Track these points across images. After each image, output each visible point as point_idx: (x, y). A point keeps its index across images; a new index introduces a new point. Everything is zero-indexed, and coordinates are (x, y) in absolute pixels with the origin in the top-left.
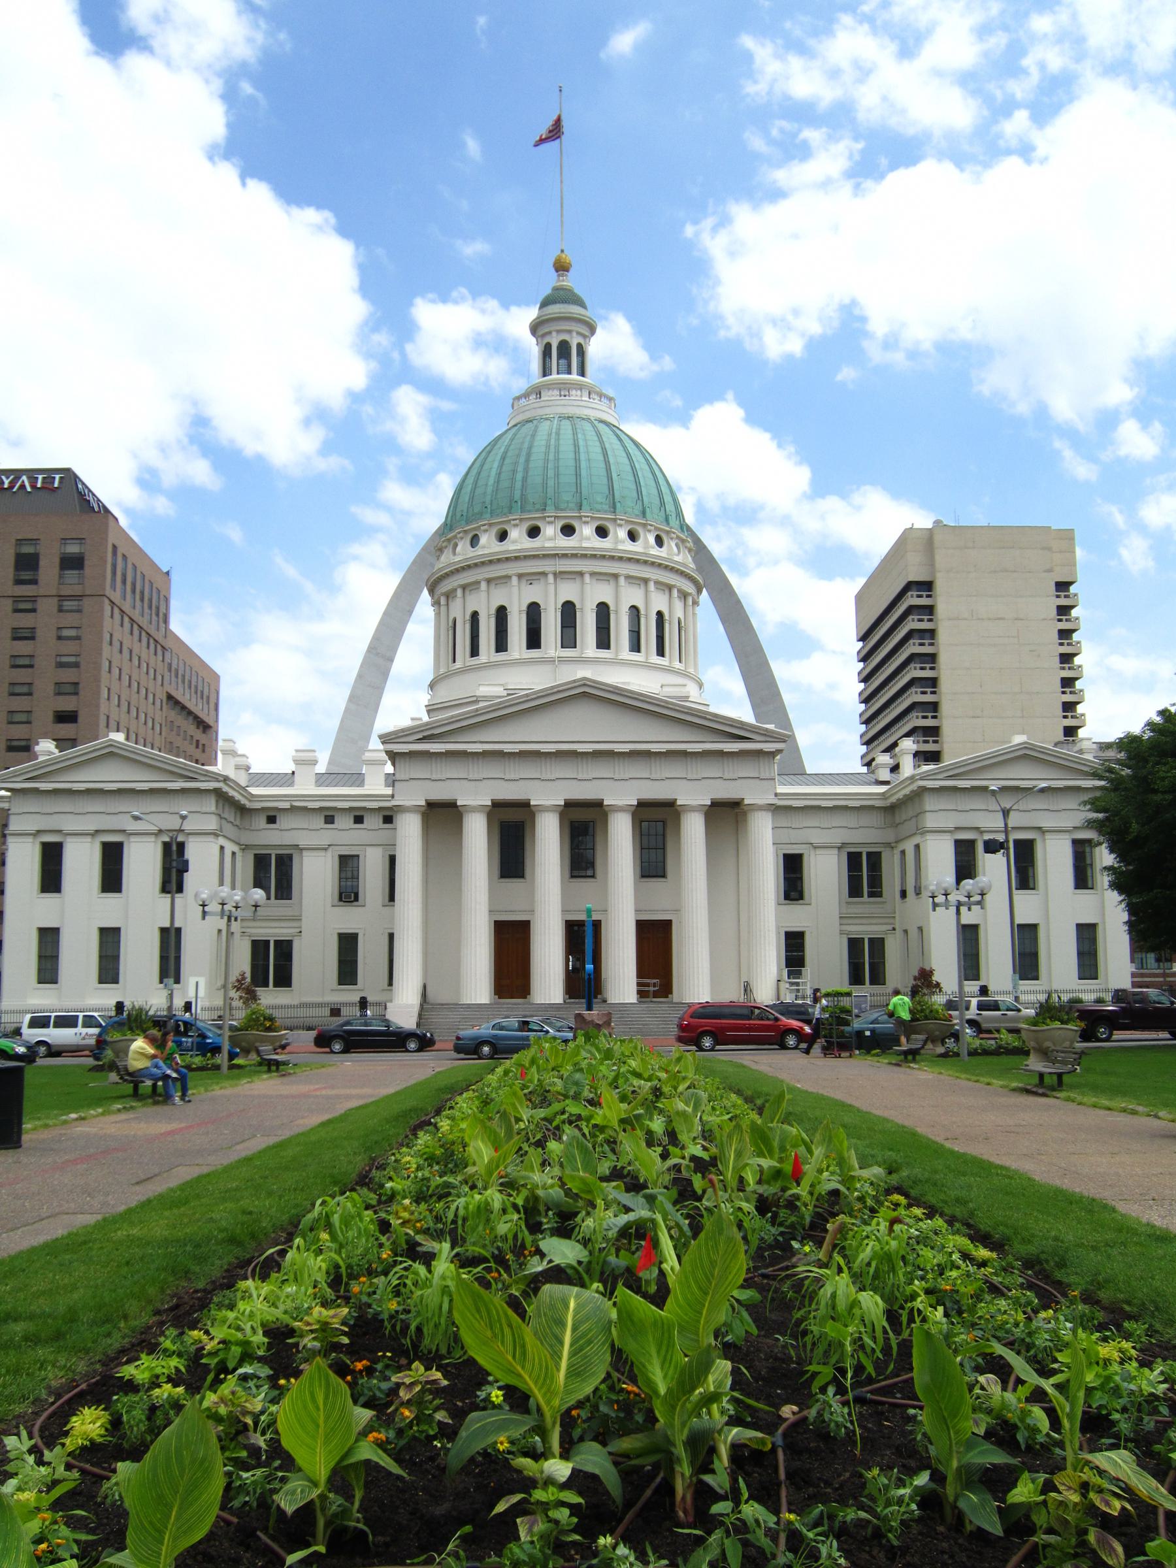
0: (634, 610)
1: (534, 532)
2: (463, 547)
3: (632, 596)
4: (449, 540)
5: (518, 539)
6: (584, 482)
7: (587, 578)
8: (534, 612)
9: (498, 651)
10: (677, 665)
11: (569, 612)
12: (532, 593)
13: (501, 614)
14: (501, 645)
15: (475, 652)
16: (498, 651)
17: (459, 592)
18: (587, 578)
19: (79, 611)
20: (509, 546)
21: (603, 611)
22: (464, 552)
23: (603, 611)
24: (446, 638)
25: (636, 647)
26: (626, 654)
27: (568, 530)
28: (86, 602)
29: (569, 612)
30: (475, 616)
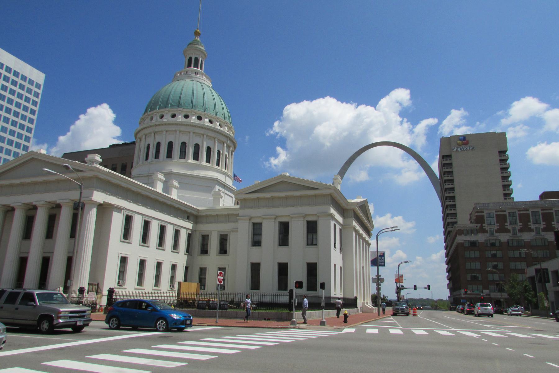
1: (174, 116)
2: (148, 120)
4: (143, 119)
6: (194, 100)
7: (191, 134)
9: (155, 158)
11: (184, 145)
12: (170, 138)
13: (158, 145)
16: (155, 158)
17: (144, 137)
18: (191, 134)
20: (165, 120)
22: (147, 122)
25: (208, 161)
27: (186, 117)
30: (149, 146)
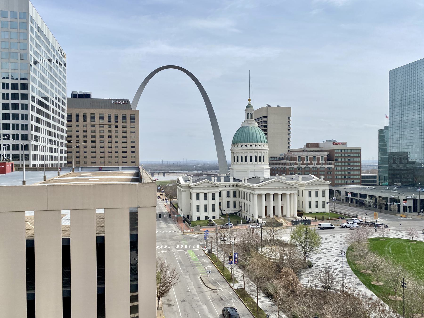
0: (260, 156)
3: (260, 154)
5: (244, 146)
8: (246, 157)
10: (263, 163)
13: (242, 157)
14: (242, 161)
15: (238, 161)
19: (134, 128)
21: (256, 157)
23: (256, 157)
24: (233, 158)
25: (260, 161)
26: (259, 163)
27: (251, 146)
28: (136, 126)
29: (251, 157)
